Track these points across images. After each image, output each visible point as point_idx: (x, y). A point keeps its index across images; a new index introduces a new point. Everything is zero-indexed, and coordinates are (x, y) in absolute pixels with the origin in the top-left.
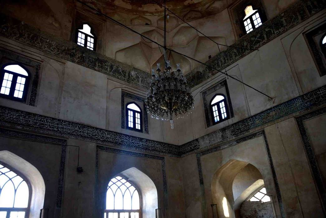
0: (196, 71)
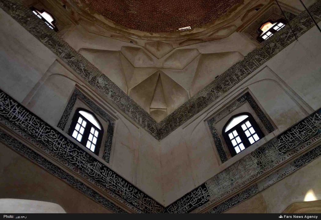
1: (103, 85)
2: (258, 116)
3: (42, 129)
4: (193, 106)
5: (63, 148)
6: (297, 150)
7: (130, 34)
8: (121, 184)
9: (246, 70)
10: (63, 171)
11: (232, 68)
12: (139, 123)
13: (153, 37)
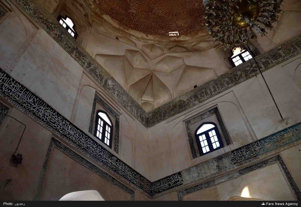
0: (178, 100)
1: (111, 87)
2: (221, 128)
3: (83, 139)
4: (175, 106)
5: (95, 150)
6: (242, 164)
7: (130, 35)
8: (127, 170)
9: (218, 88)
10: (97, 167)
11: (208, 83)
12: (134, 116)
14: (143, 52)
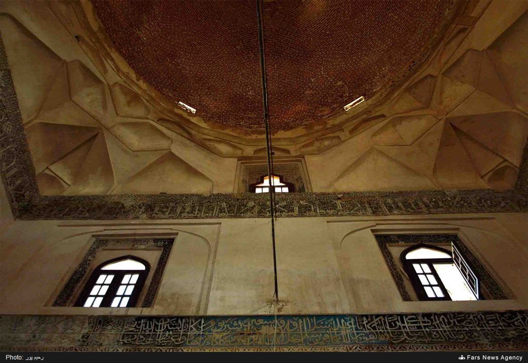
0: (116, 199)
4: (100, 207)
7: (108, 55)
9: (199, 210)
13: (137, 85)
14: (111, 92)
